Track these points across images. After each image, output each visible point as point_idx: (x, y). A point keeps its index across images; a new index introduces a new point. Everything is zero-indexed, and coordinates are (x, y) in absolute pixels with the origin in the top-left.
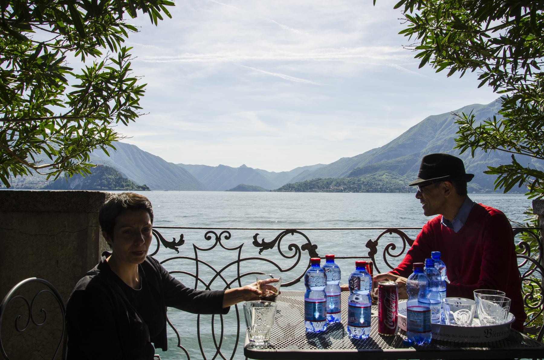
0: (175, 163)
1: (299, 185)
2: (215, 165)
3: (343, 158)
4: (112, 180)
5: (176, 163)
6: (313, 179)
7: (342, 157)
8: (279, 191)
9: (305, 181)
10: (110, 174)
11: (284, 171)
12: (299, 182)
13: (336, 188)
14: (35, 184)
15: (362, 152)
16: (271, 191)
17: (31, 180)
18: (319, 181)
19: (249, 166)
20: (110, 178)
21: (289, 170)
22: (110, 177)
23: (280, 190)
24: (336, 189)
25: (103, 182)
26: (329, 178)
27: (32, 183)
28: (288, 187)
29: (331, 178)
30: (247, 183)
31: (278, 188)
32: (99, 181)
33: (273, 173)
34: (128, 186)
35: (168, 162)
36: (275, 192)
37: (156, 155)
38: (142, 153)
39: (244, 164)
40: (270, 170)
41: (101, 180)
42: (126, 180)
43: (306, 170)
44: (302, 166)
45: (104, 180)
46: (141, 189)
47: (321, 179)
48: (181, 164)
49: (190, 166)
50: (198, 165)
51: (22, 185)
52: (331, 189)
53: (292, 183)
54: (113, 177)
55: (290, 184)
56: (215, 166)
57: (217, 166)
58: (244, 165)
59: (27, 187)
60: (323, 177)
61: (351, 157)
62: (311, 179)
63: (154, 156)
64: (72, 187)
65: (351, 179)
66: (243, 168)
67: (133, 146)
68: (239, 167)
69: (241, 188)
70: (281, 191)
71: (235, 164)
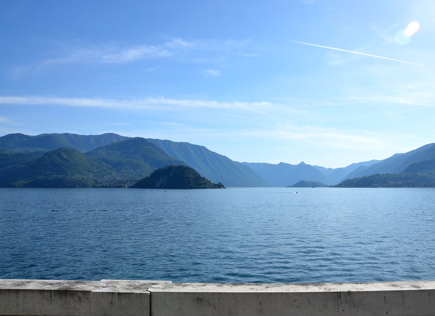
0: (240, 162)
1: (358, 180)
2: (276, 162)
3: (397, 154)
5: (240, 161)
6: (371, 175)
7: (396, 153)
8: (339, 187)
9: (364, 177)
11: (341, 167)
12: (358, 178)
13: (394, 183)
15: (416, 148)
16: (331, 187)
17: (120, 179)
18: (378, 176)
19: (307, 163)
21: (345, 167)
23: (340, 185)
24: (395, 184)
26: (387, 174)
27: (119, 183)
28: (348, 183)
29: (389, 174)
30: (307, 179)
31: (338, 184)
33: (330, 169)
35: (234, 161)
36: (336, 187)
37: (223, 155)
39: (303, 161)
40: (327, 167)
43: (361, 166)
44: (357, 162)
47: (378, 175)
48: (245, 163)
49: (253, 164)
50: (260, 163)
52: (389, 184)
53: (351, 178)
55: (349, 180)
56: (276, 164)
57: (278, 163)
58: (303, 162)
60: (381, 173)
61: (404, 152)
62: (370, 175)
65: (408, 174)
66: (302, 165)
67: (202, 146)
68: (298, 164)
69: (302, 184)
70: (342, 187)
71: (295, 162)
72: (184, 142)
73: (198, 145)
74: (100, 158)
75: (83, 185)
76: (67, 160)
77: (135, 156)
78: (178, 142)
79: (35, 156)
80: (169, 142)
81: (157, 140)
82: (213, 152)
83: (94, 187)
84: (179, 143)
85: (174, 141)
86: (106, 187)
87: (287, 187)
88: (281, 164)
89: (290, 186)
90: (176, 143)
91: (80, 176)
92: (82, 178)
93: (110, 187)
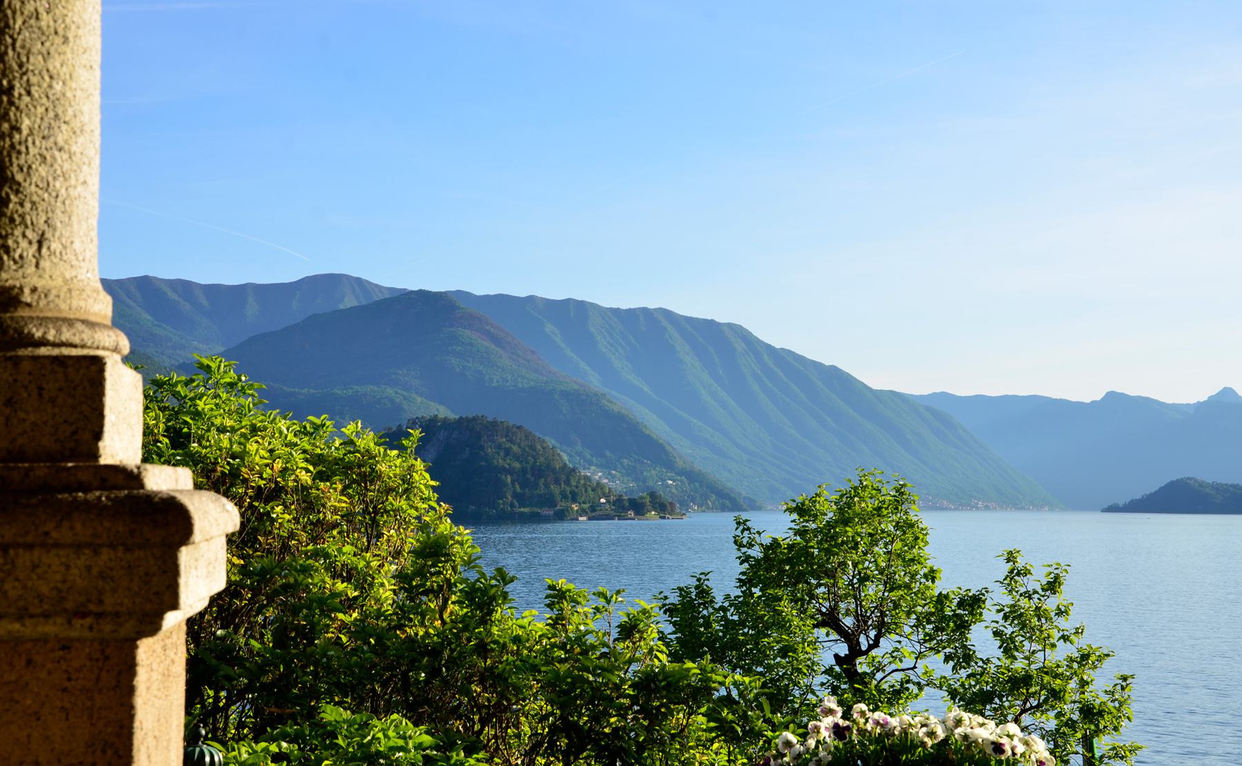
37: (827, 362)
38: (766, 358)
63: (817, 366)
67: (731, 326)
68: (1204, 398)
72: (652, 305)
73: (712, 320)
77: (400, 372)
78: (624, 306)
80: (580, 308)
81: (531, 299)
82: (782, 349)
84: (631, 312)
85: (608, 300)
87: (1102, 511)
88: (1112, 397)
89: (1121, 504)
90: (616, 311)
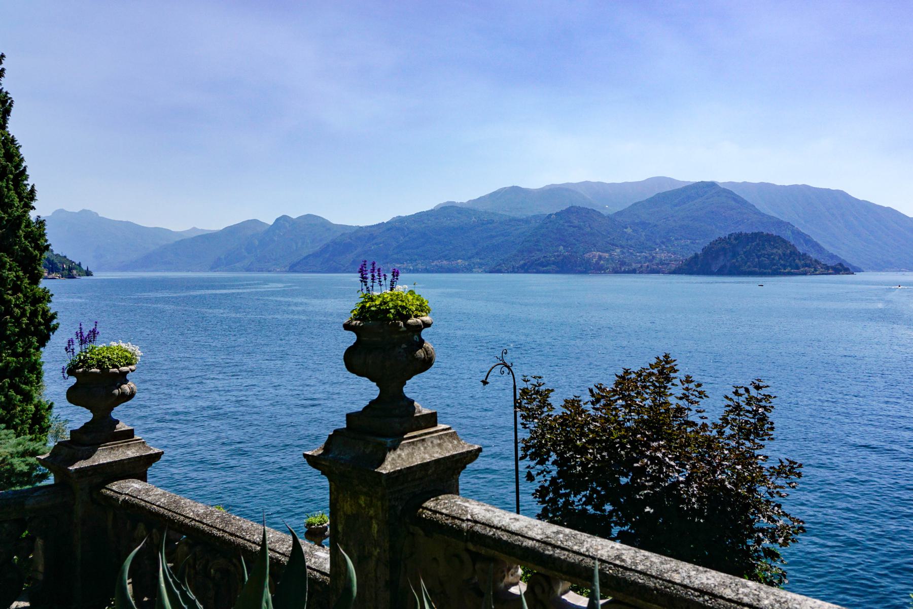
4: (777, 258)
10: (776, 247)
14: (666, 264)
20: (772, 254)
22: (775, 251)
25: (762, 261)
32: (756, 260)
34: (806, 265)
41: (759, 257)
42: (804, 256)
45: (764, 257)
46: (831, 271)
51: (648, 266)
54: (780, 252)
59: (654, 269)
64: (713, 269)
74: (636, 221)
75: (598, 269)
76: (580, 228)
79: (533, 222)
83: (616, 272)
86: (633, 271)
91: (598, 253)
92: (600, 258)
93: (641, 272)
